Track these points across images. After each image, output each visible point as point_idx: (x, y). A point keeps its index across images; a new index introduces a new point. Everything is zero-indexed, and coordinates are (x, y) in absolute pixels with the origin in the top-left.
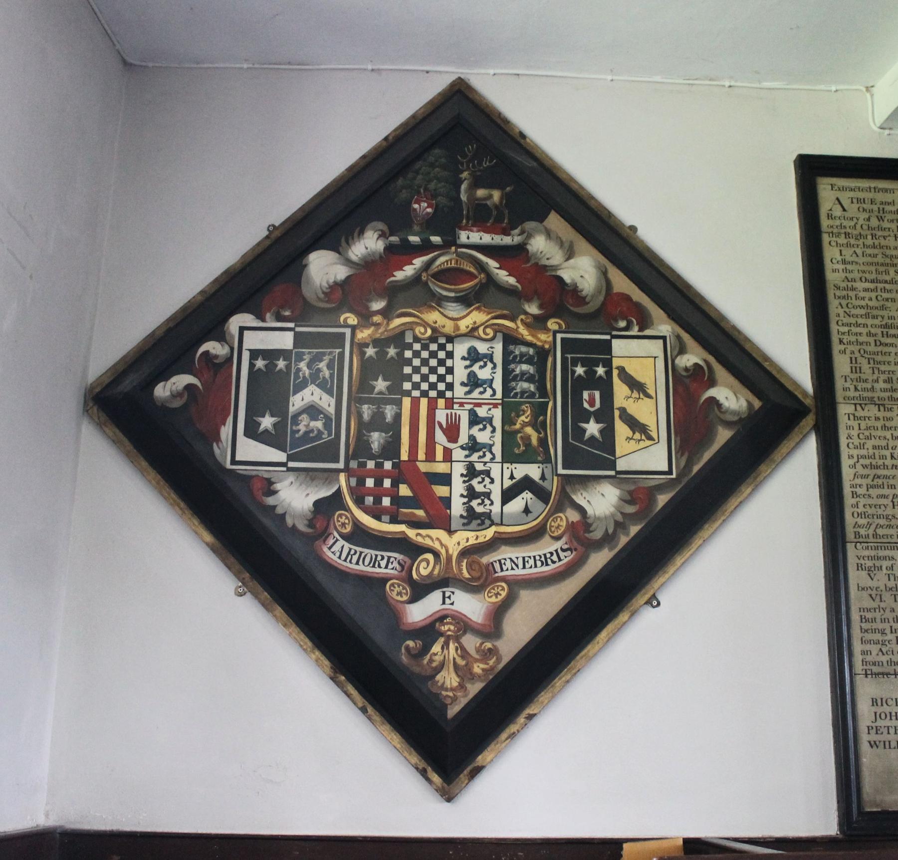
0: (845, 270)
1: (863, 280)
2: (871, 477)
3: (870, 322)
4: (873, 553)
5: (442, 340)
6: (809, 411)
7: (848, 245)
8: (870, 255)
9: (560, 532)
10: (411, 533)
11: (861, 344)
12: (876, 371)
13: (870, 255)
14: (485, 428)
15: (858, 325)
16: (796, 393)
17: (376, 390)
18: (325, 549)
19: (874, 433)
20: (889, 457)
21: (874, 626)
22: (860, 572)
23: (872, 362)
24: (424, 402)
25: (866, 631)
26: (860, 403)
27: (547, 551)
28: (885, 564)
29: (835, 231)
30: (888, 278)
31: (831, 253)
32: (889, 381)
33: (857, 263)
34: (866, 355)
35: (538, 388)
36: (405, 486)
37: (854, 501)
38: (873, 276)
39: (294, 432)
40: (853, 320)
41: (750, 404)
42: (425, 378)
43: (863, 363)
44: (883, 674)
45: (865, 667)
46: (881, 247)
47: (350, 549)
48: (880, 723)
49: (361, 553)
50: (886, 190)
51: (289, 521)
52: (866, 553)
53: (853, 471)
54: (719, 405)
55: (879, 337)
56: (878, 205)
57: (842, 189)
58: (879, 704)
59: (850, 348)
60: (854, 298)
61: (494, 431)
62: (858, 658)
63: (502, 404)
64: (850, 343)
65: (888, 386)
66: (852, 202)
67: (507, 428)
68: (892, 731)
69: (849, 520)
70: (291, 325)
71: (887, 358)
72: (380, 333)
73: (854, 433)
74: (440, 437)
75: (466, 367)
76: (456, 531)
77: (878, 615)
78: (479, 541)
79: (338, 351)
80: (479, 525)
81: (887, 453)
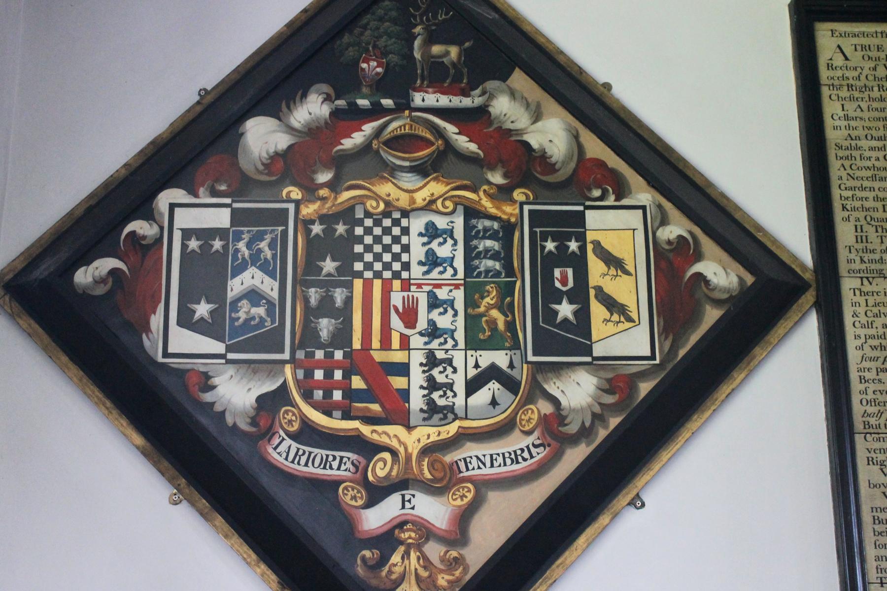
0: (848, 127)
1: (869, 137)
2: (882, 359)
3: (877, 185)
5: (396, 215)
6: (810, 286)
7: (852, 99)
9: (531, 426)
10: (366, 430)
11: (868, 210)
13: (877, 109)
14: (446, 311)
15: (863, 189)
16: (793, 266)
17: (324, 272)
22: (871, 466)
23: (880, 230)
24: (377, 284)
25: (880, 534)
26: (867, 277)
29: (836, 82)
31: (831, 108)
33: (861, 119)
35: (504, 267)
36: (358, 377)
37: (862, 387)
40: (858, 184)
41: (741, 279)
42: (378, 257)
43: (870, 231)
45: (880, 575)
47: (298, 449)
49: (310, 453)
51: (230, 420)
52: (877, 445)
53: (860, 353)
54: (707, 282)
57: (845, 35)
59: (856, 214)
60: (858, 158)
61: (456, 314)
62: (871, 564)
63: (465, 285)
64: (854, 209)
66: (856, 50)
67: (470, 311)
69: (857, 409)
70: (228, 201)
72: (327, 208)
73: (861, 310)
74: (396, 322)
75: (424, 244)
76: (416, 427)
78: (442, 437)
79: (280, 228)
80: (441, 419)
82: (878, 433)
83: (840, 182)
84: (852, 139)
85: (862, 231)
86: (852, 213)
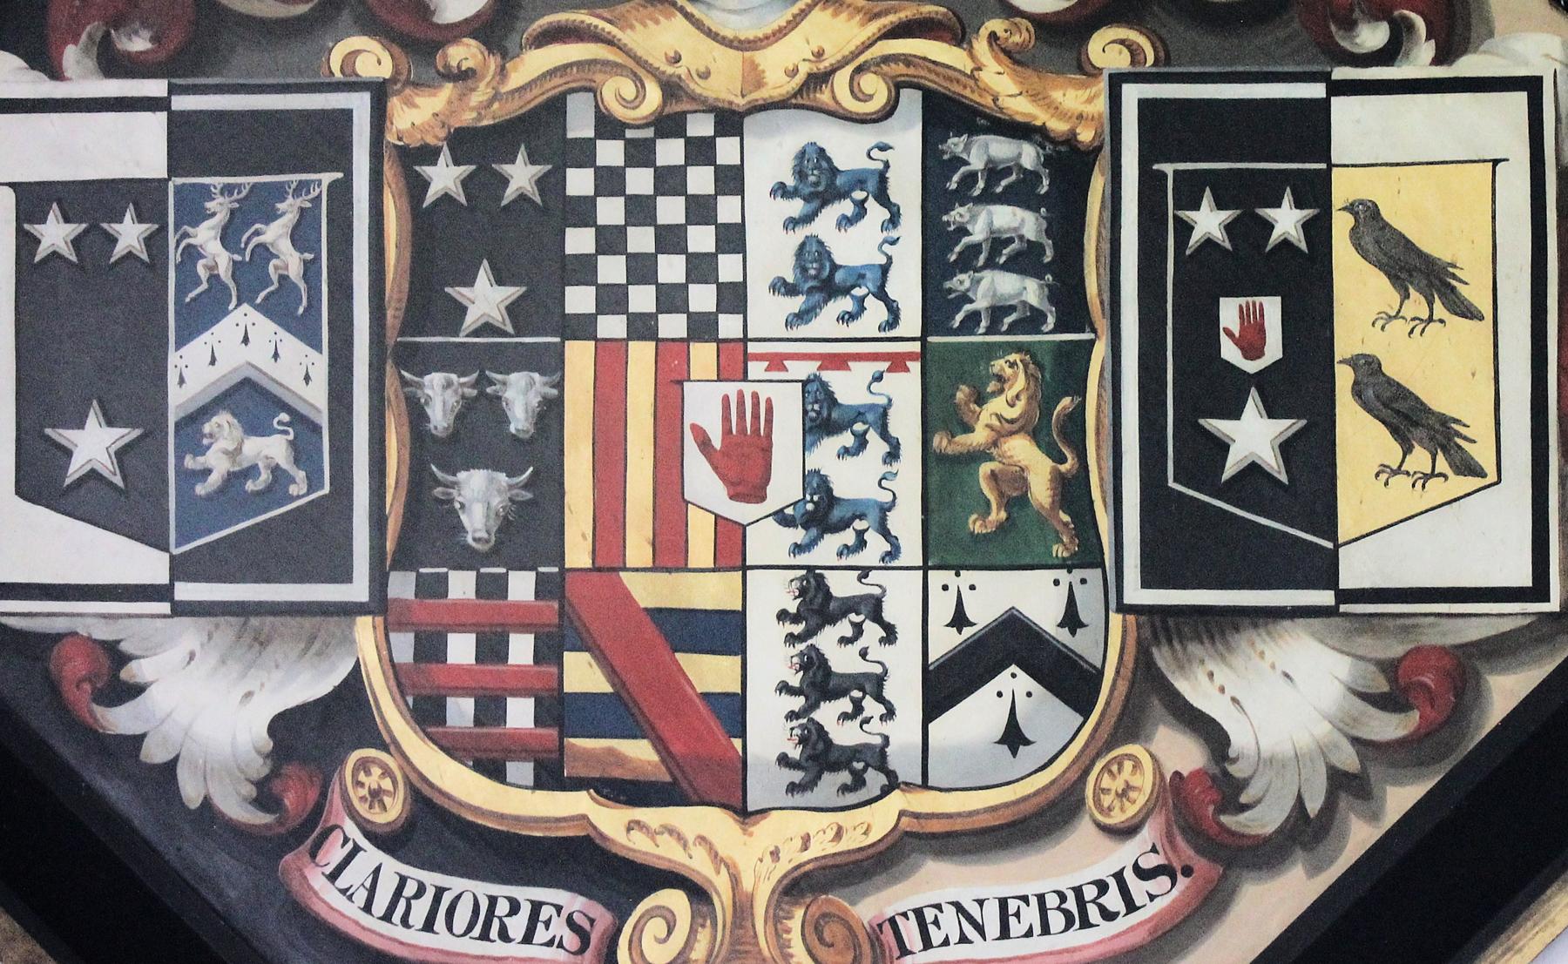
5: (701, 126)
9: (1132, 810)
10: (612, 823)
14: (862, 443)
17: (471, 320)
18: (318, 881)
24: (641, 355)
27: (1085, 876)
35: (1054, 297)
36: (585, 657)
39: (190, 478)
42: (642, 270)
47: (403, 880)
49: (440, 891)
51: (191, 791)
61: (893, 455)
63: (923, 356)
67: (940, 441)
70: (156, 88)
72: (477, 107)
74: (703, 484)
75: (792, 223)
76: (763, 812)
78: (846, 844)
79: (327, 178)
80: (845, 789)
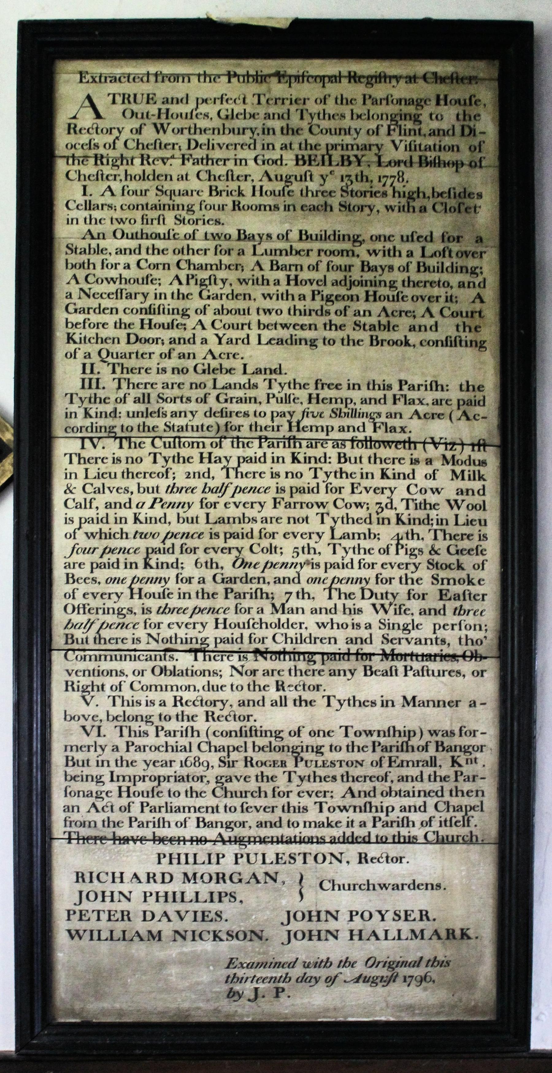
0: (89, 220)
1: (119, 235)
2: (99, 551)
3: (121, 304)
4: (91, 665)
7: (99, 177)
8: (135, 192)
11: (104, 341)
12: (124, 385)
13: (135, 192)
15: (101, 310)
19: (109, 483)
20: (131, 519)
21: (86, 771)
22: (70, 692)
23: (118, 369)
25: (74, 778)
26: (90, 437)
28: (109, 681)
29: (79, 153)
30: (161, 230)
32: (145, 399)
33: (110, 207)
34: (110, 359)
37: (68, 588)
38: (138, 227)
40: (93, 303)
43: (105, 372)
44: (95, 838)
46: (156, 177)
48: (86, 905)
50: (176, 78)
52: (81, 666)
53: (71, 542)
55: (136, 329)
56: (159, 105)
58: (87, 879)
60: (99, 266)
64: (85, 340)
65: (141, 407)
66: (114, 102)
68: (104, 916)
69: (59, 617)
71: (145, 363)
73: (77, 484)
77: (92, 756)
81: (129, 514)
82: (84, 650)
83: (68, 301)
84: (93, 238)
85: (92, 372)
86: (81, 346)
